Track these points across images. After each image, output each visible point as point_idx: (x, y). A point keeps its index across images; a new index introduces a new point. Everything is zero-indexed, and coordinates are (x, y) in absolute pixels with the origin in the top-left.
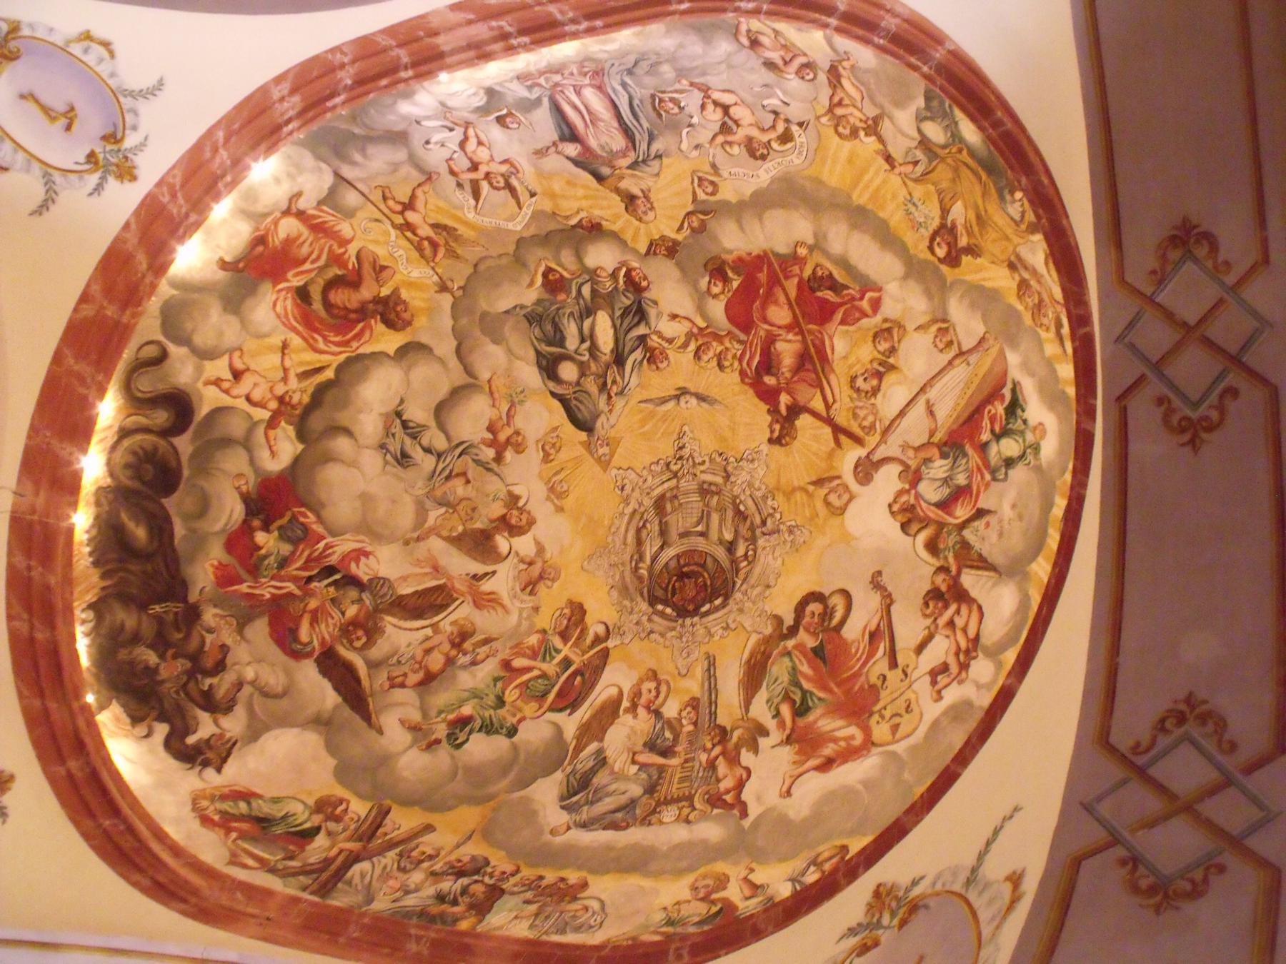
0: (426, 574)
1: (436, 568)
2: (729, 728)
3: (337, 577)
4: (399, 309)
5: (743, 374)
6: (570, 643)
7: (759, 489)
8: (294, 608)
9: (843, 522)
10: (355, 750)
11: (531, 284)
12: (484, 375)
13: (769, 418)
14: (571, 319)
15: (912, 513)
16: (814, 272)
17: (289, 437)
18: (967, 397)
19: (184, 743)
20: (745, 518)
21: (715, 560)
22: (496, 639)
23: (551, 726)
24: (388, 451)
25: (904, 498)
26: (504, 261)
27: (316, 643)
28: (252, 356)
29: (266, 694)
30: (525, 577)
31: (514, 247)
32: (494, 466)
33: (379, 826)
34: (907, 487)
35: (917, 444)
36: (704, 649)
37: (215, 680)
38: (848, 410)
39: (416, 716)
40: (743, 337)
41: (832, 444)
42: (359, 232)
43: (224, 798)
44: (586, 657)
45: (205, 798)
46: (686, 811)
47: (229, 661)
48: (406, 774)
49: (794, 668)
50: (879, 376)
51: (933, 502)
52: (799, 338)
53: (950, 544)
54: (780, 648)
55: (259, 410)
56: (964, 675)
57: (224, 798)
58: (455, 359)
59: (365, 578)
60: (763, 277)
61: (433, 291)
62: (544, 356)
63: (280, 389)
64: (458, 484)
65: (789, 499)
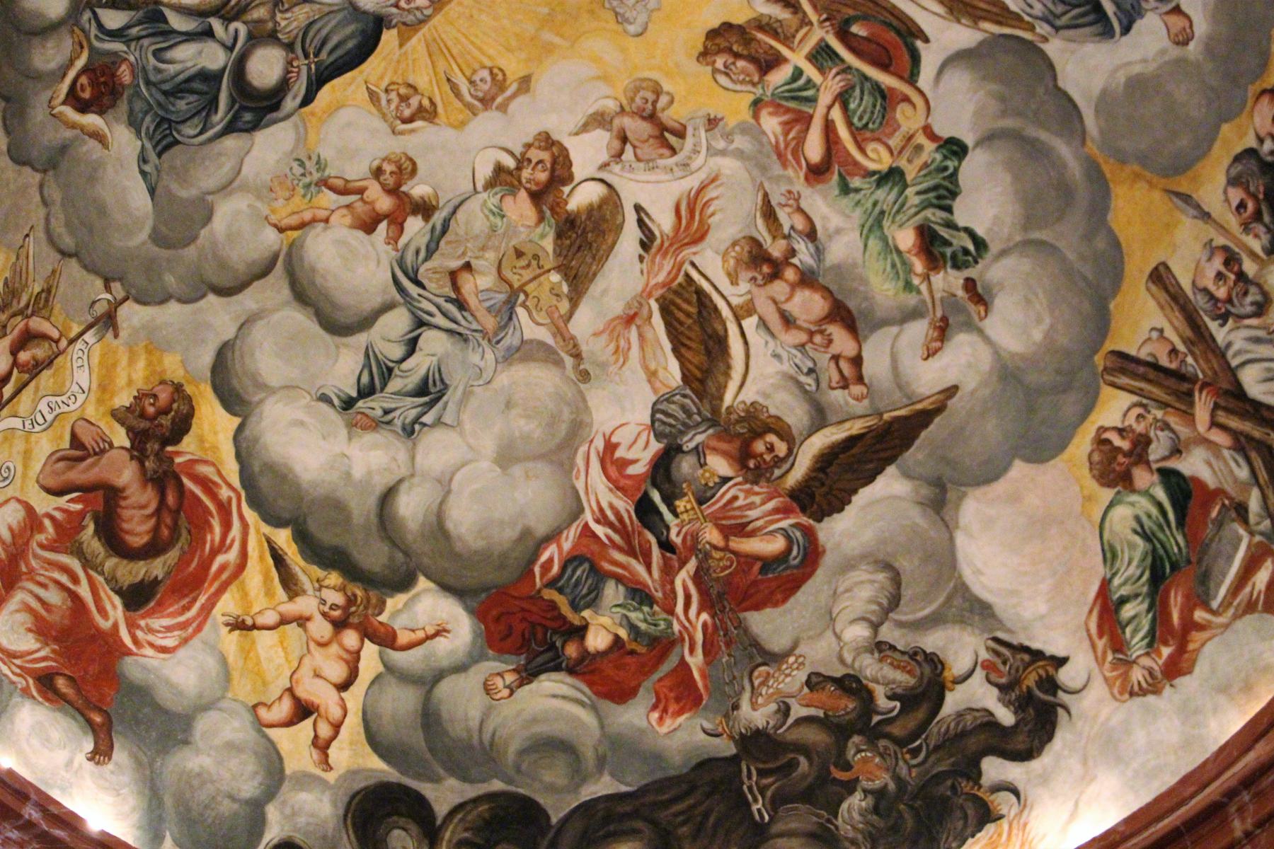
0: (641, 337)
1: (629, 320)
3: (656, 496)
4: (151, 410)
6: (785, 51)
8: (721, 566)
10: (991, 432)
11: (98, 136)
12: (271, 238)
14: (169, 55)
17: (406, 604)
22: (766, 195)
23: (946, 76)
24: (416, 420)
26: (55, 194)
27: (784, 524)
28: (265, 684)
29: (895, 601)
30: (647, 150)
31: (27, 170)
32: (438, 218)
33: (1155, 366)
37: (880, 693)
39: (918, 330)
42: (10, 492)
43: (1118, 645)
44: (813, 16)
45: (1125, 677)
47: (839, 672)
48: (1037, 335)
55: (362, 665)
57: (1118, 645)
58: (240, 297)
59: (656, 446)
61: (116, 342)
62: (235, 118)
63: (321, 628)
64: (468, 285)
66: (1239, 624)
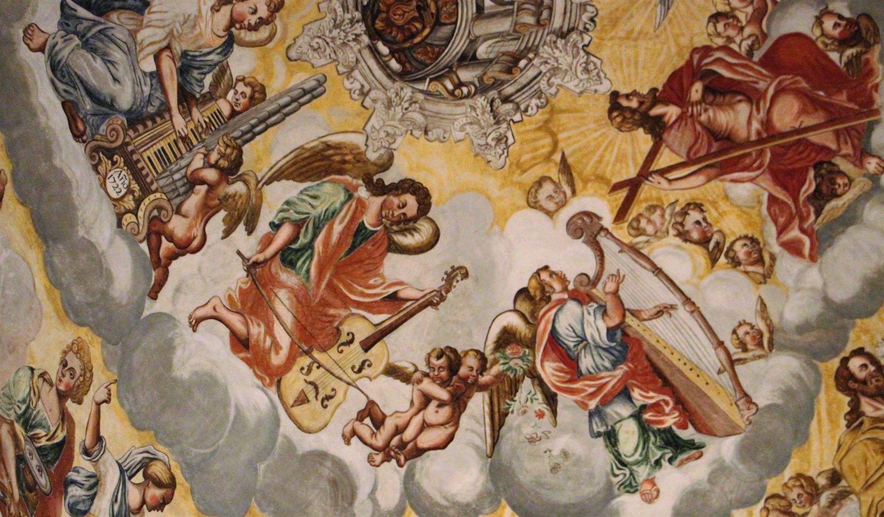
2: (242, 170)
5: (707, 50)
7: (550, 85)
9: (519, 208)
13: (645, 91)
15: (541, 299)
16: (842, 174)
18: (679, 364)
20: (509, 71)
21: (449, 39)
25: (557, 286)
34: (571, 287)
35: (621, 293)
36: (330, 71)
38: (659, 199)
40: (757, 56)
41: (615, 180)
46: (129, 203)
49: (334, 214)
50: (704, 242)
51: (557, 326)
52: (753, 137)
53: (512, 363)
54: (355, 181)
56: (378, 458)
60: (842, 99)
65: (539, 129)
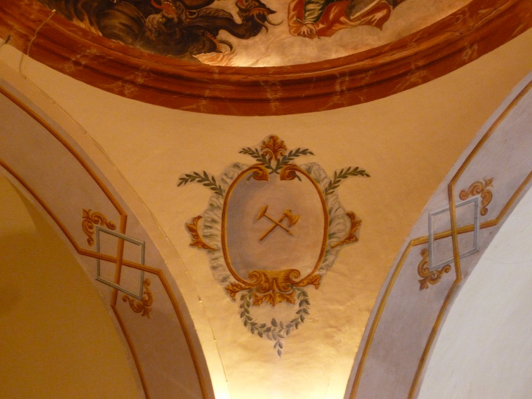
19: (241, 25)
66: (361, 27)
